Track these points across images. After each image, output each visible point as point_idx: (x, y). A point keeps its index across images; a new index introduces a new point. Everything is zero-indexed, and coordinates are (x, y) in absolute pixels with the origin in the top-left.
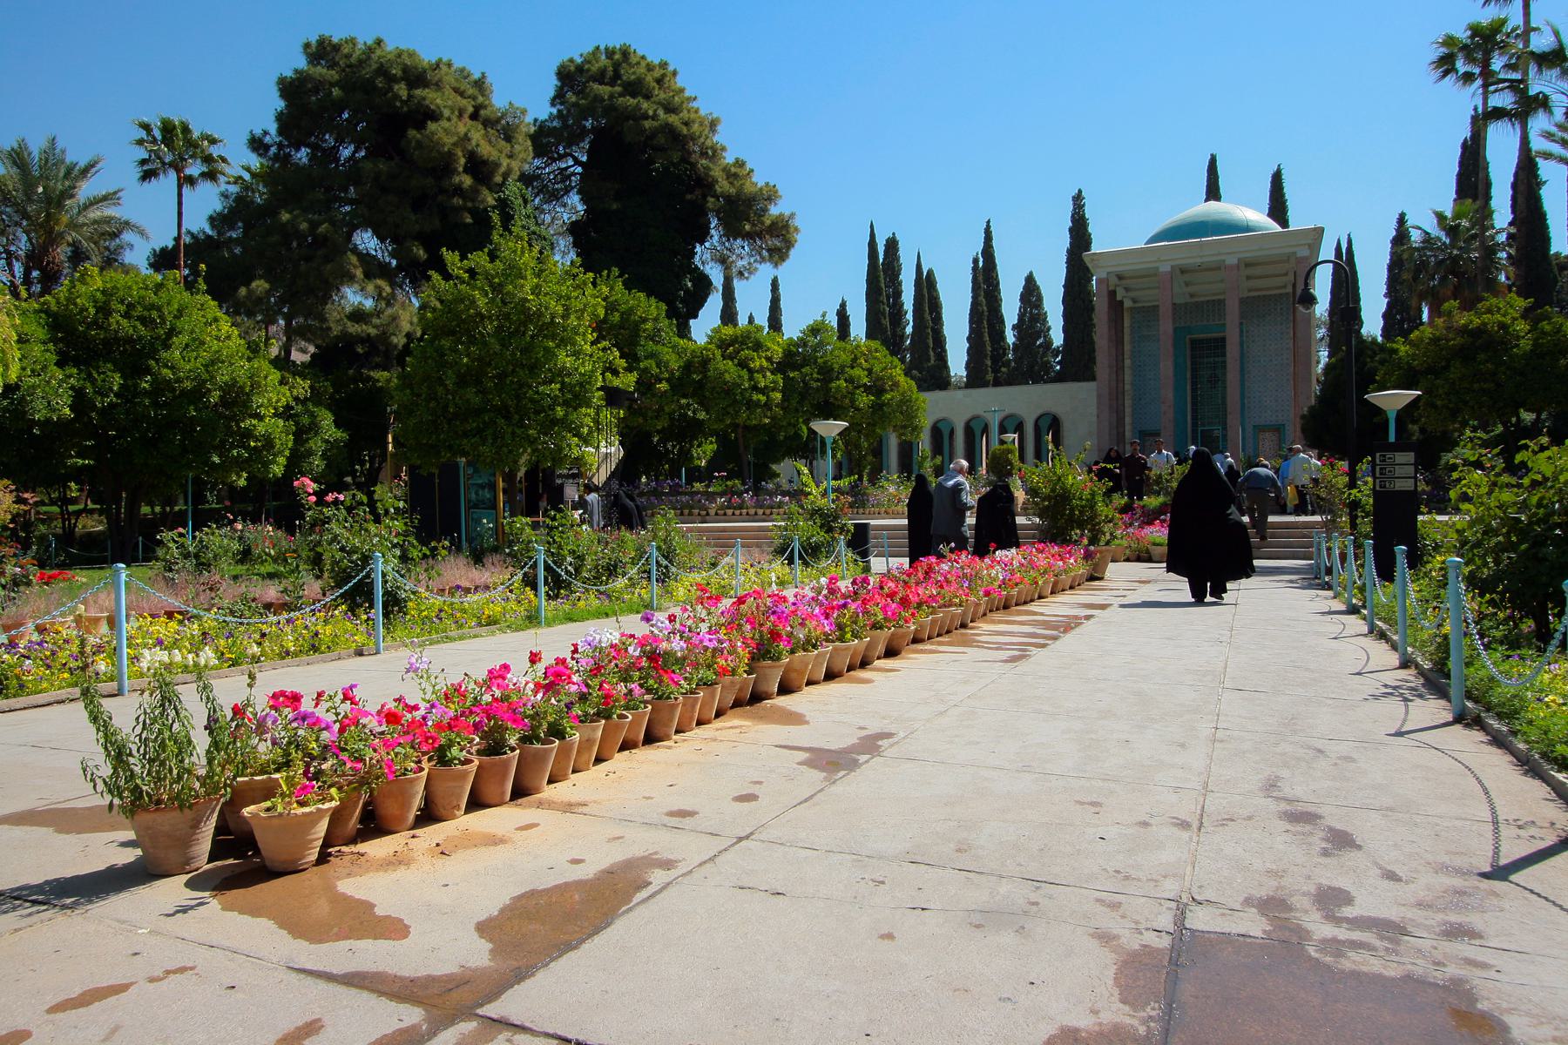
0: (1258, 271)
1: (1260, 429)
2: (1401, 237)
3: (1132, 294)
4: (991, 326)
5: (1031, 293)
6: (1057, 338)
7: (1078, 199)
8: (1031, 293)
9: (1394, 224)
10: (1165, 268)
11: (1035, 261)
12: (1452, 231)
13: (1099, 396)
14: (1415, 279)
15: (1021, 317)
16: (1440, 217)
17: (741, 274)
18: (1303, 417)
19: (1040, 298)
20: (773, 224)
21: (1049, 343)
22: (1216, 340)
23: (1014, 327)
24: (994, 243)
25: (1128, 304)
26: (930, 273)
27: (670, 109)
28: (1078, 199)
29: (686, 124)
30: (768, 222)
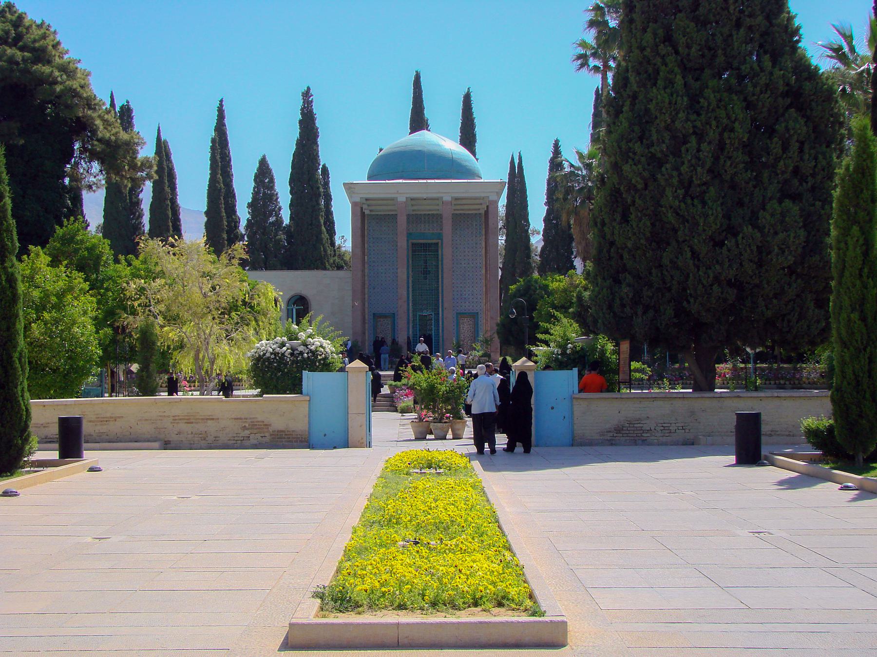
0: (464, 202)
1: (460, 315)
2: (556, 164)
3: (371, 208)
4: (226, 203)
5: (264, 174)
6: (286, 216)
7: (307, 94)
8: (264, 174)
9: (551, 148)
10: (402, 199)
11: (264, 144)
12: (588, 166)
13: (354, 291)
14: (565, 199)
15: (256, 194)
16: (581, 156)
17: (90, 187)
18: (498, 325)
19: (272, 181)
20: (142, 164)
21: (279, 221)
22: (430, 245)
23: (250, 205)
24: (226, 121)
25: (367, 212)
26: (166, 142)
27: (65, 69)
28: (307, 94)
29: (82, 87)
30: (139, 164)
